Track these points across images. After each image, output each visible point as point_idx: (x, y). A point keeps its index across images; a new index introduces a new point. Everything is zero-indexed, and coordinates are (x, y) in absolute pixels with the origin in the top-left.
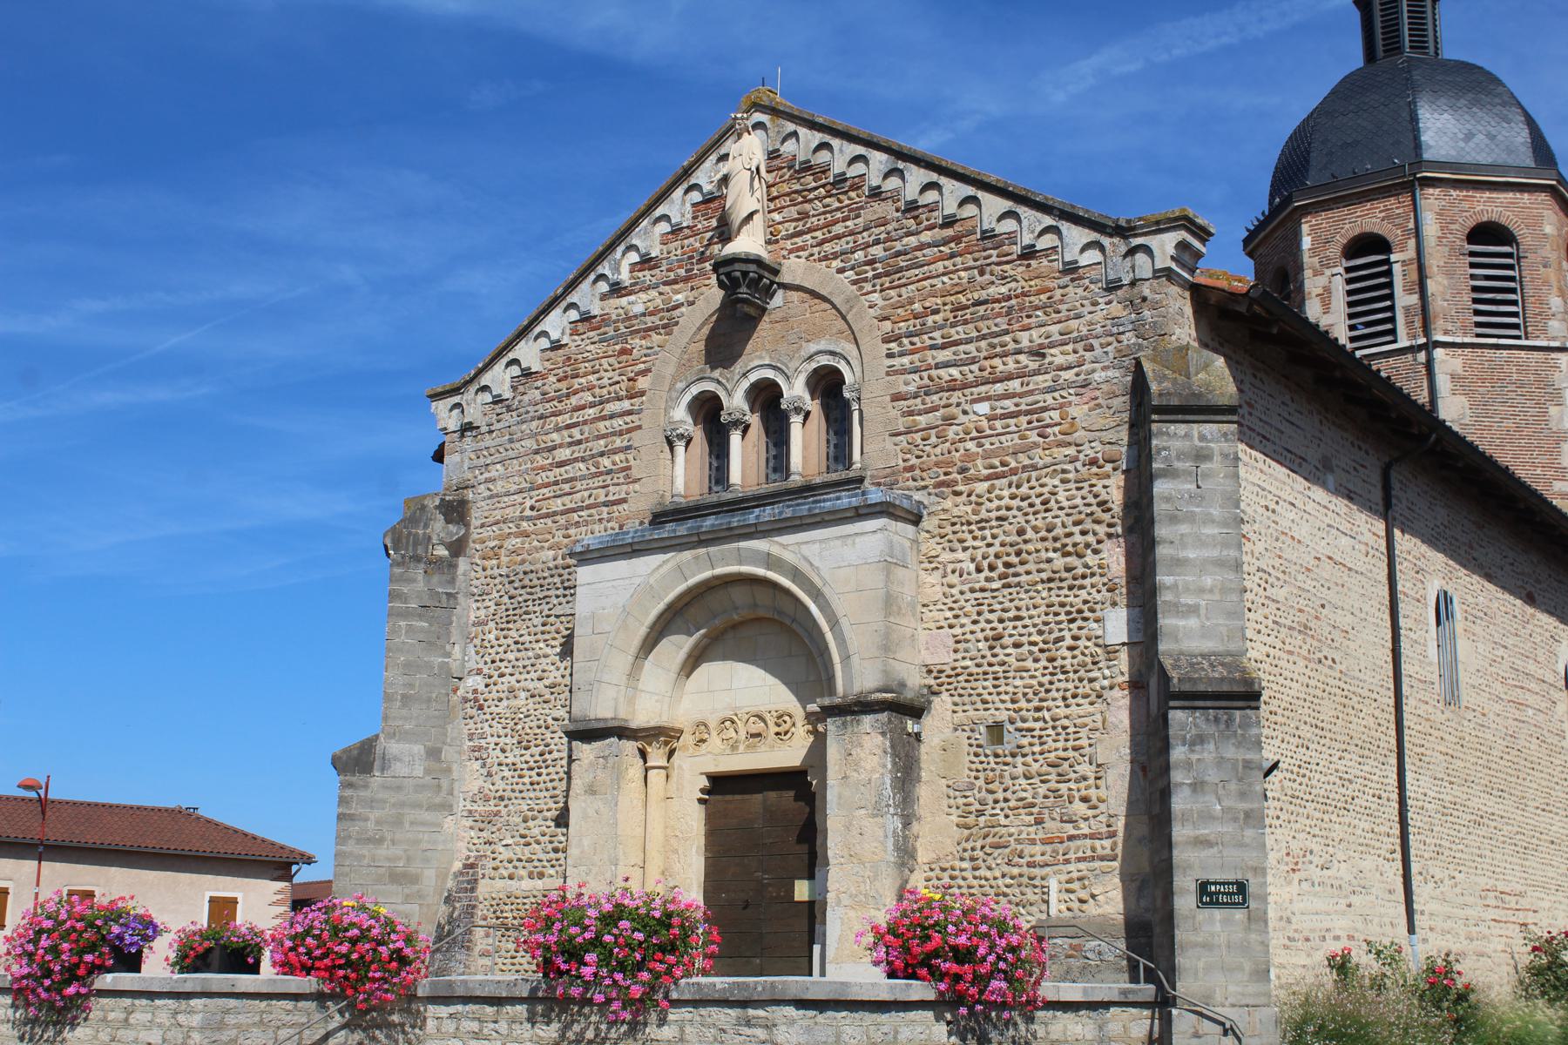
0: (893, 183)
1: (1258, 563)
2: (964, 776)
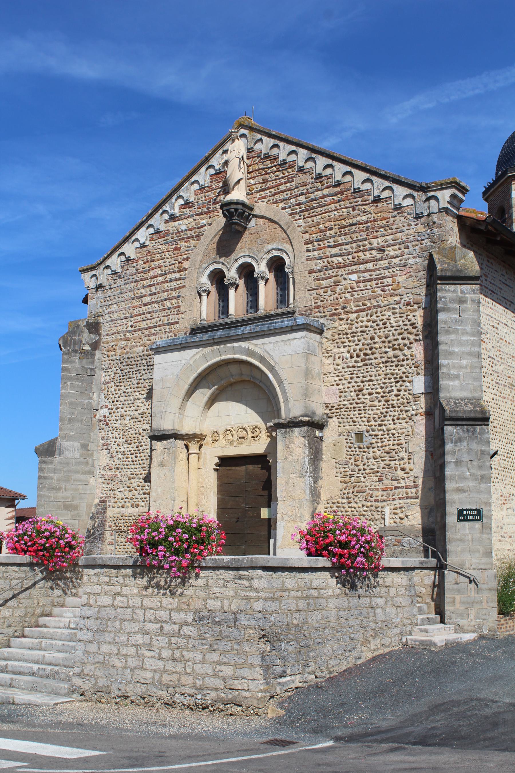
0: (310, 164)
1: (488, 354)
2: (344, 458)
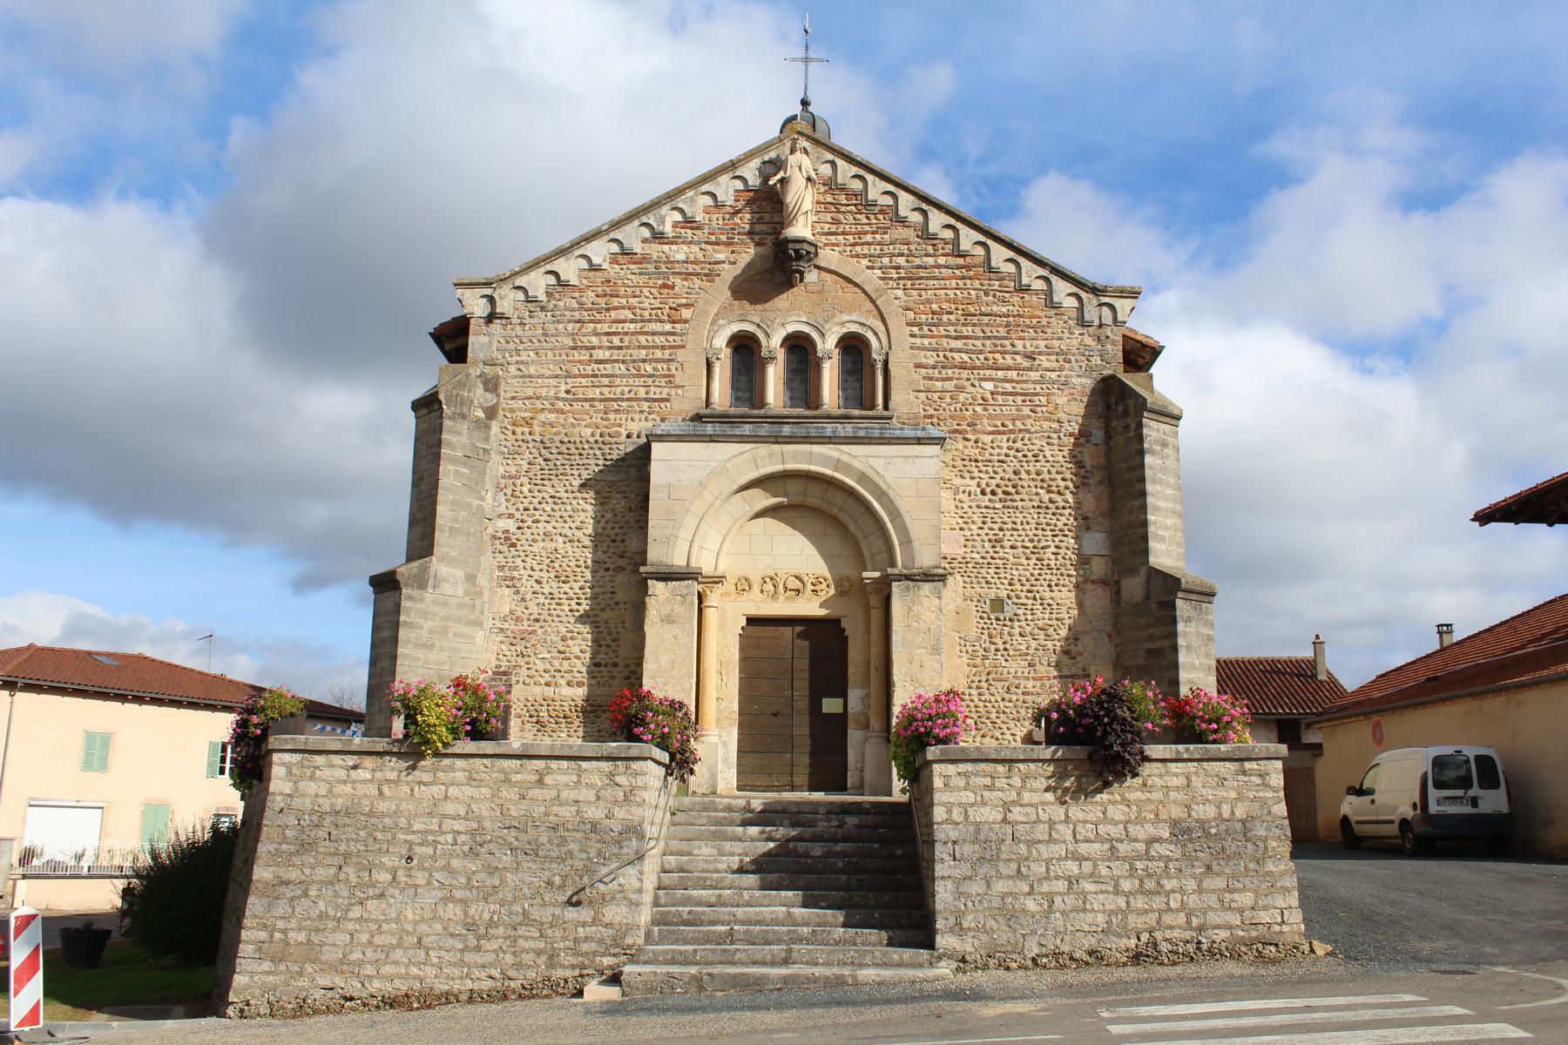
2: (973, 633)
